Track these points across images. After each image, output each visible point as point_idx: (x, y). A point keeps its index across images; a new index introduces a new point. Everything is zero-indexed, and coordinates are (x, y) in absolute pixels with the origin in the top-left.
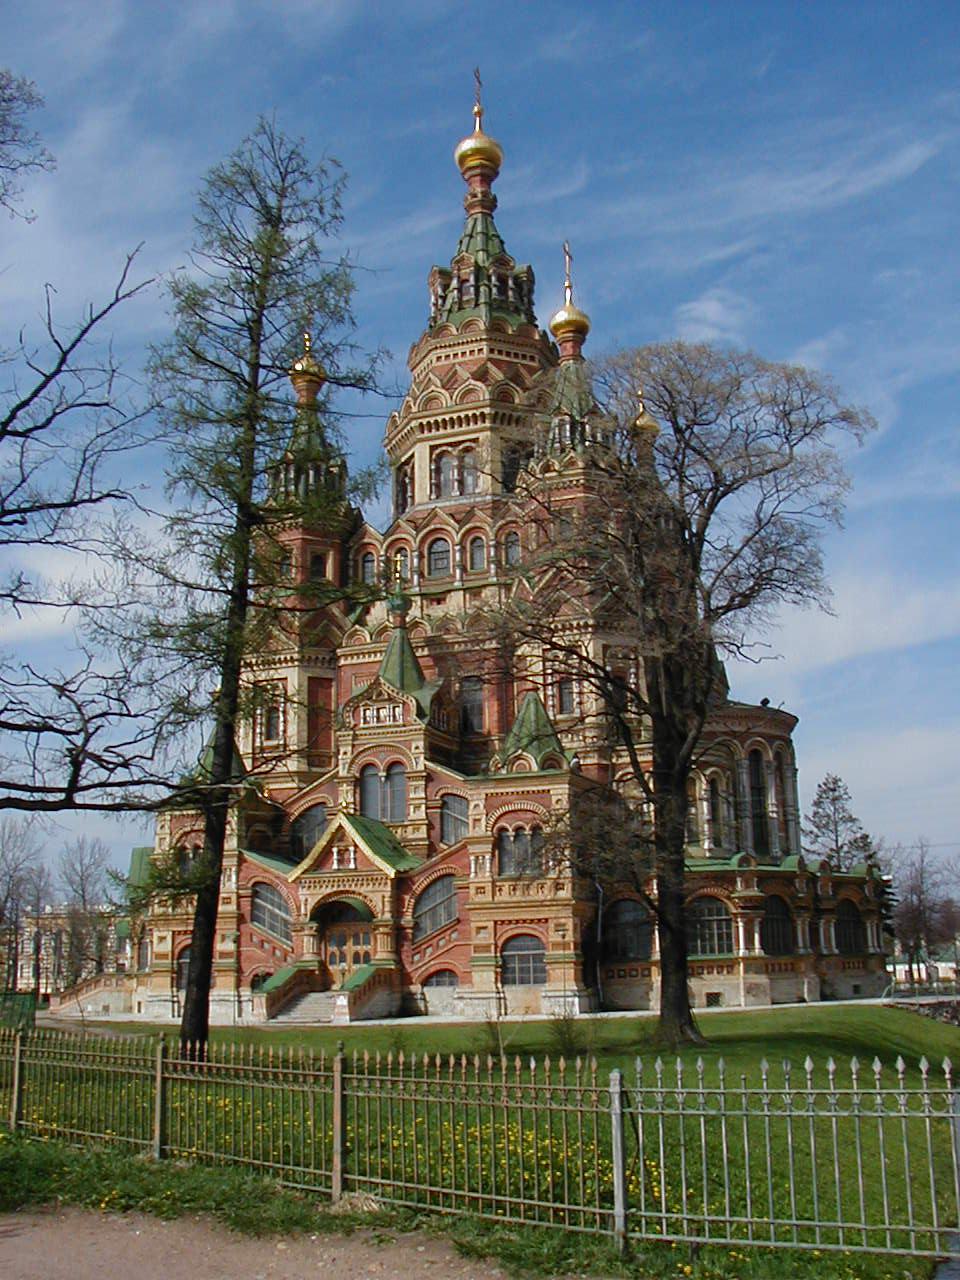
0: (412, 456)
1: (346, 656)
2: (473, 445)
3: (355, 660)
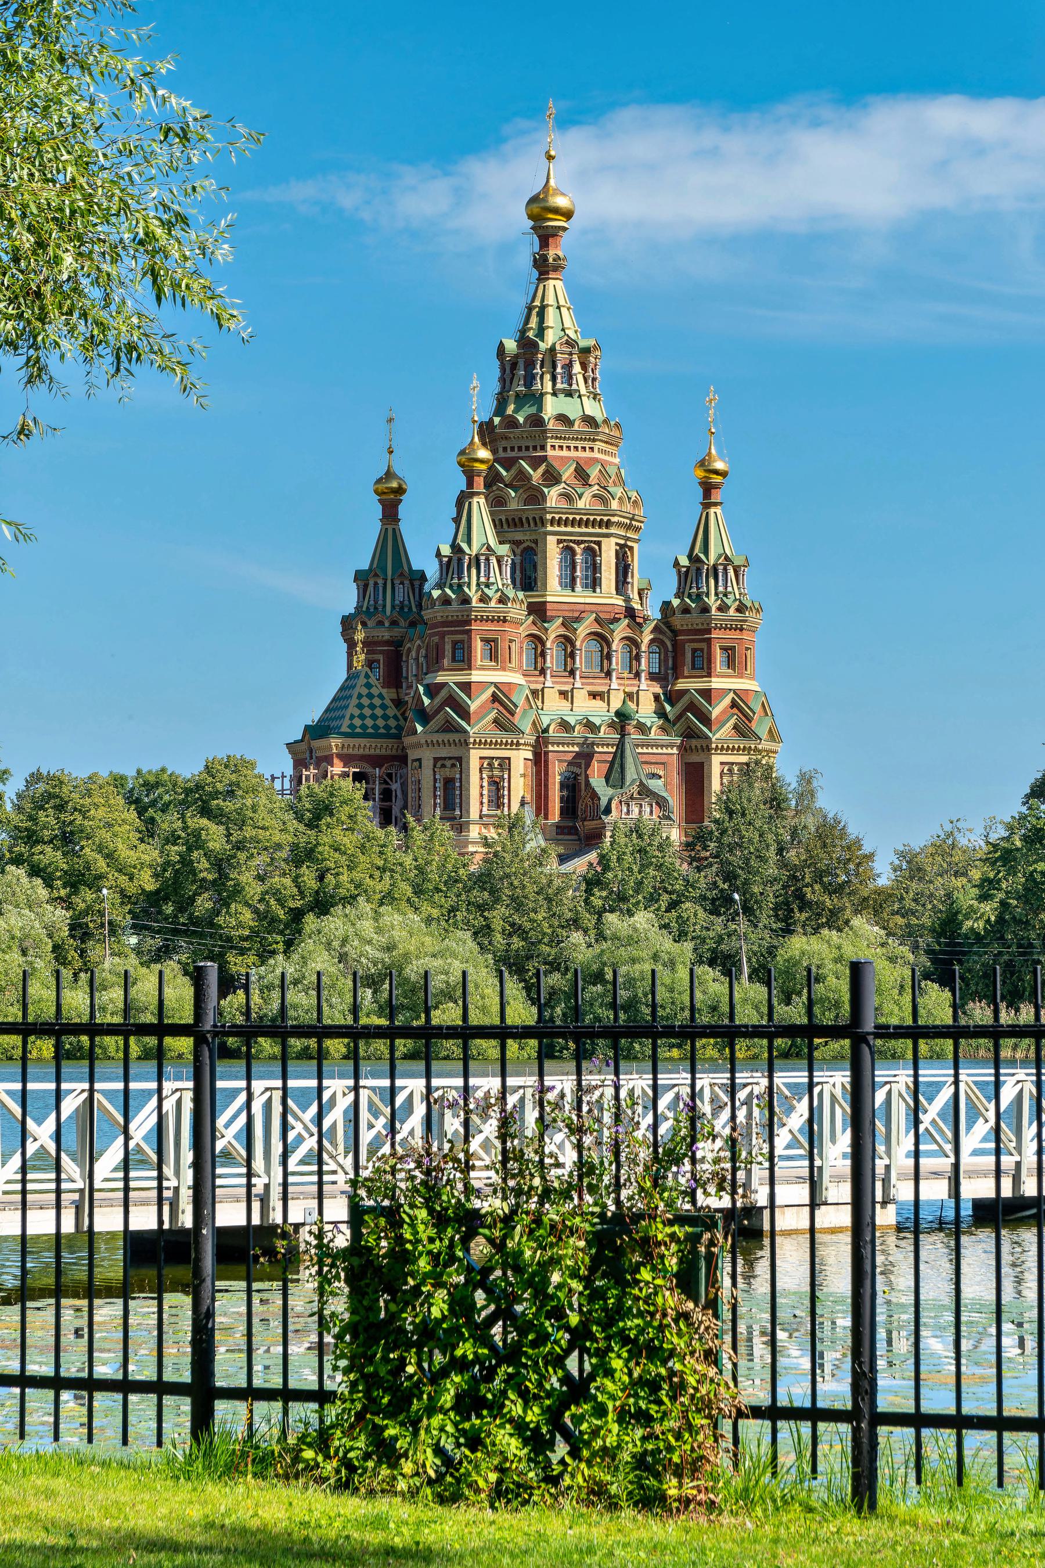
0: (536, 542)
1: (553, 744)
3: (561, 748)
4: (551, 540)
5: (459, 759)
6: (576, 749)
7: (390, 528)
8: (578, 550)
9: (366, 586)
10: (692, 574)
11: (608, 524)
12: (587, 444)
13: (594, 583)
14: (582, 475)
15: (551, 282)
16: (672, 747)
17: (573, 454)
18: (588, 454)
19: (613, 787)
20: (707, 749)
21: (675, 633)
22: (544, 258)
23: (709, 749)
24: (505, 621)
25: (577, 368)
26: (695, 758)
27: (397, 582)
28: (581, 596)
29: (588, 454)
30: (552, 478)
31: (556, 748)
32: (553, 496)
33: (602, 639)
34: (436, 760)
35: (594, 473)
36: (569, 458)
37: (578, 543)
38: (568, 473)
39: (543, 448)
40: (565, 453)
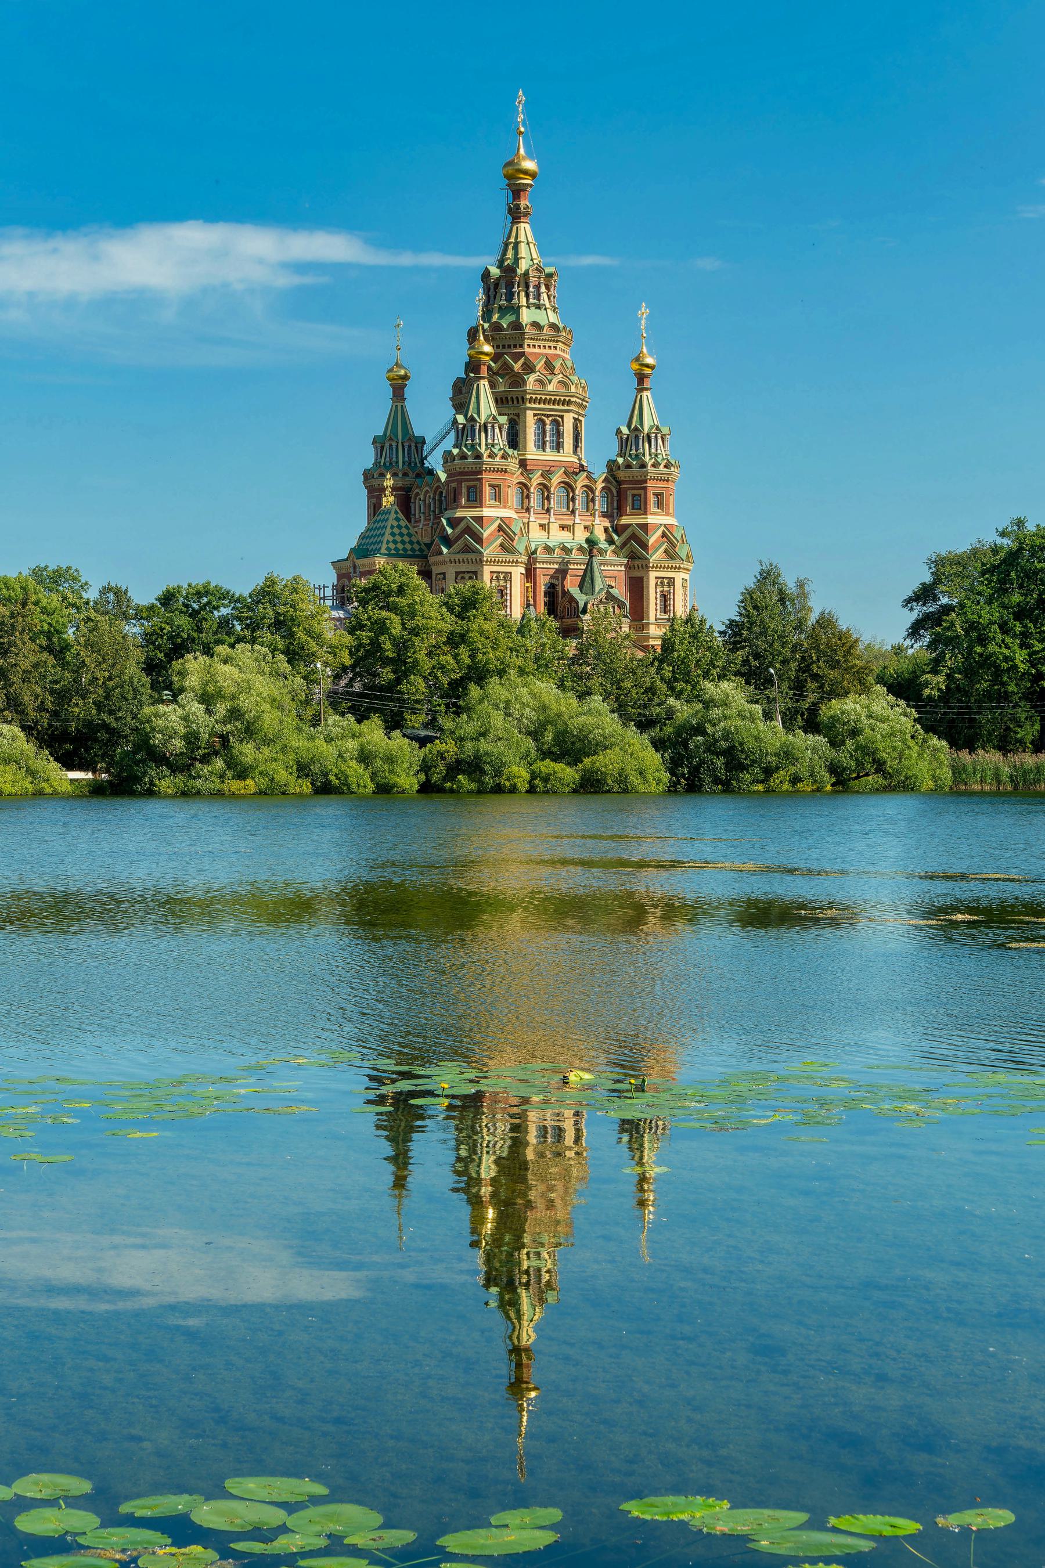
0: (518, 415)
3: (545, 566)
4: (529, 414)
5: (475, 573)
6: (556, 566)
7: (399, 405)
8: (548, 421)
9: (382, 447)
10: (631, 440)
11: (569, 403)
12: (552, 344)
13: (558, 446)
14: (549, 366)
15: (522, 225)
16: (621, 565)
17: (542, 351)
18: (552, 351)
19: (586, 594)
20: (646, 567)
21: (619, 483)
22: (518, 207)
23: (647, 567)
24: (506, 472)
25: (543, 289)
26: (637, 574)
27: (406, 445)
28: (550, 455)
29: (552, 351)
30: (529, 368)
31: (542, 566)
32: (531, 380)
33: (568, 487)
34: (457, 573)
35: (557, 364)
36: (540, 354)
37: (548, 416)
38: (540, 365)
39: (521, 346)
40: (537, 350)
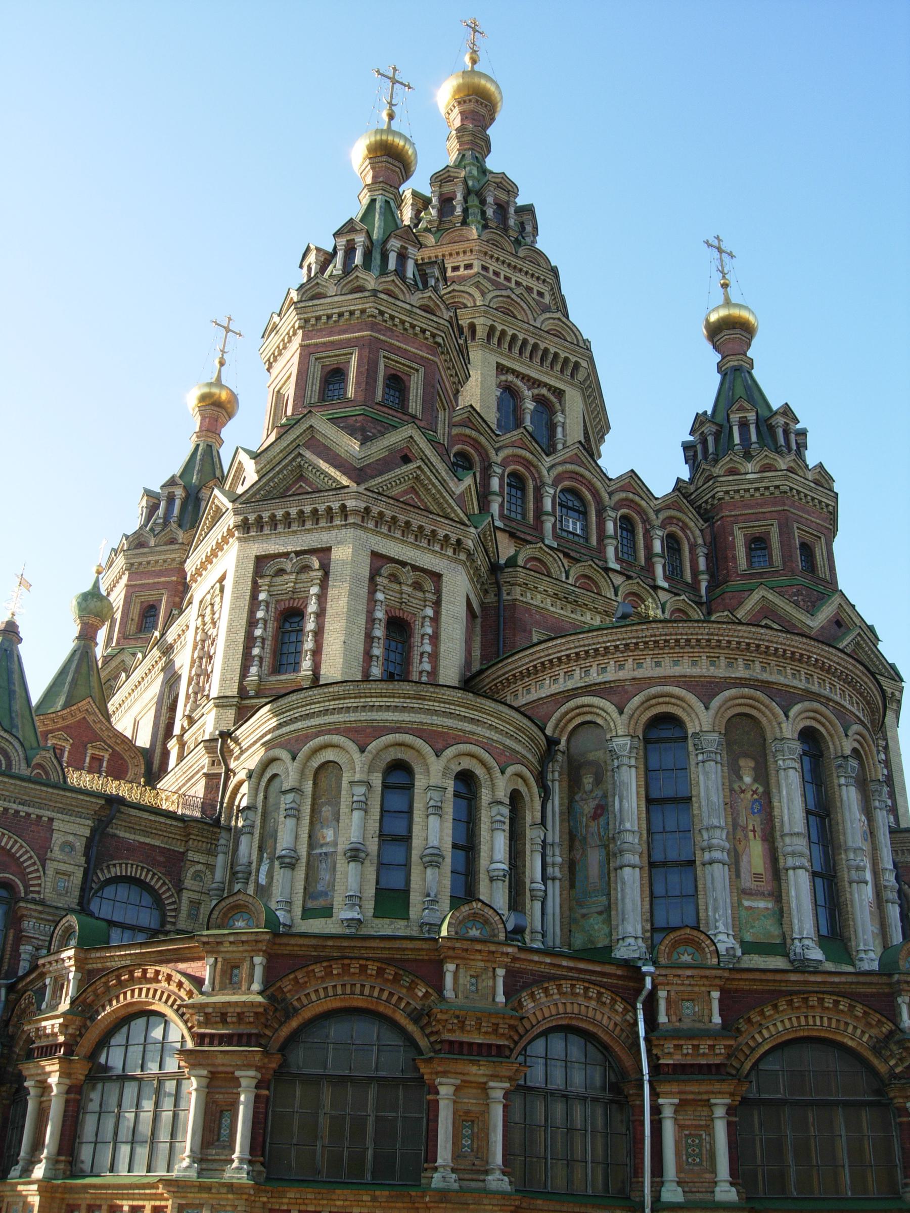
2: (553, 398)
8: (528, 393)
